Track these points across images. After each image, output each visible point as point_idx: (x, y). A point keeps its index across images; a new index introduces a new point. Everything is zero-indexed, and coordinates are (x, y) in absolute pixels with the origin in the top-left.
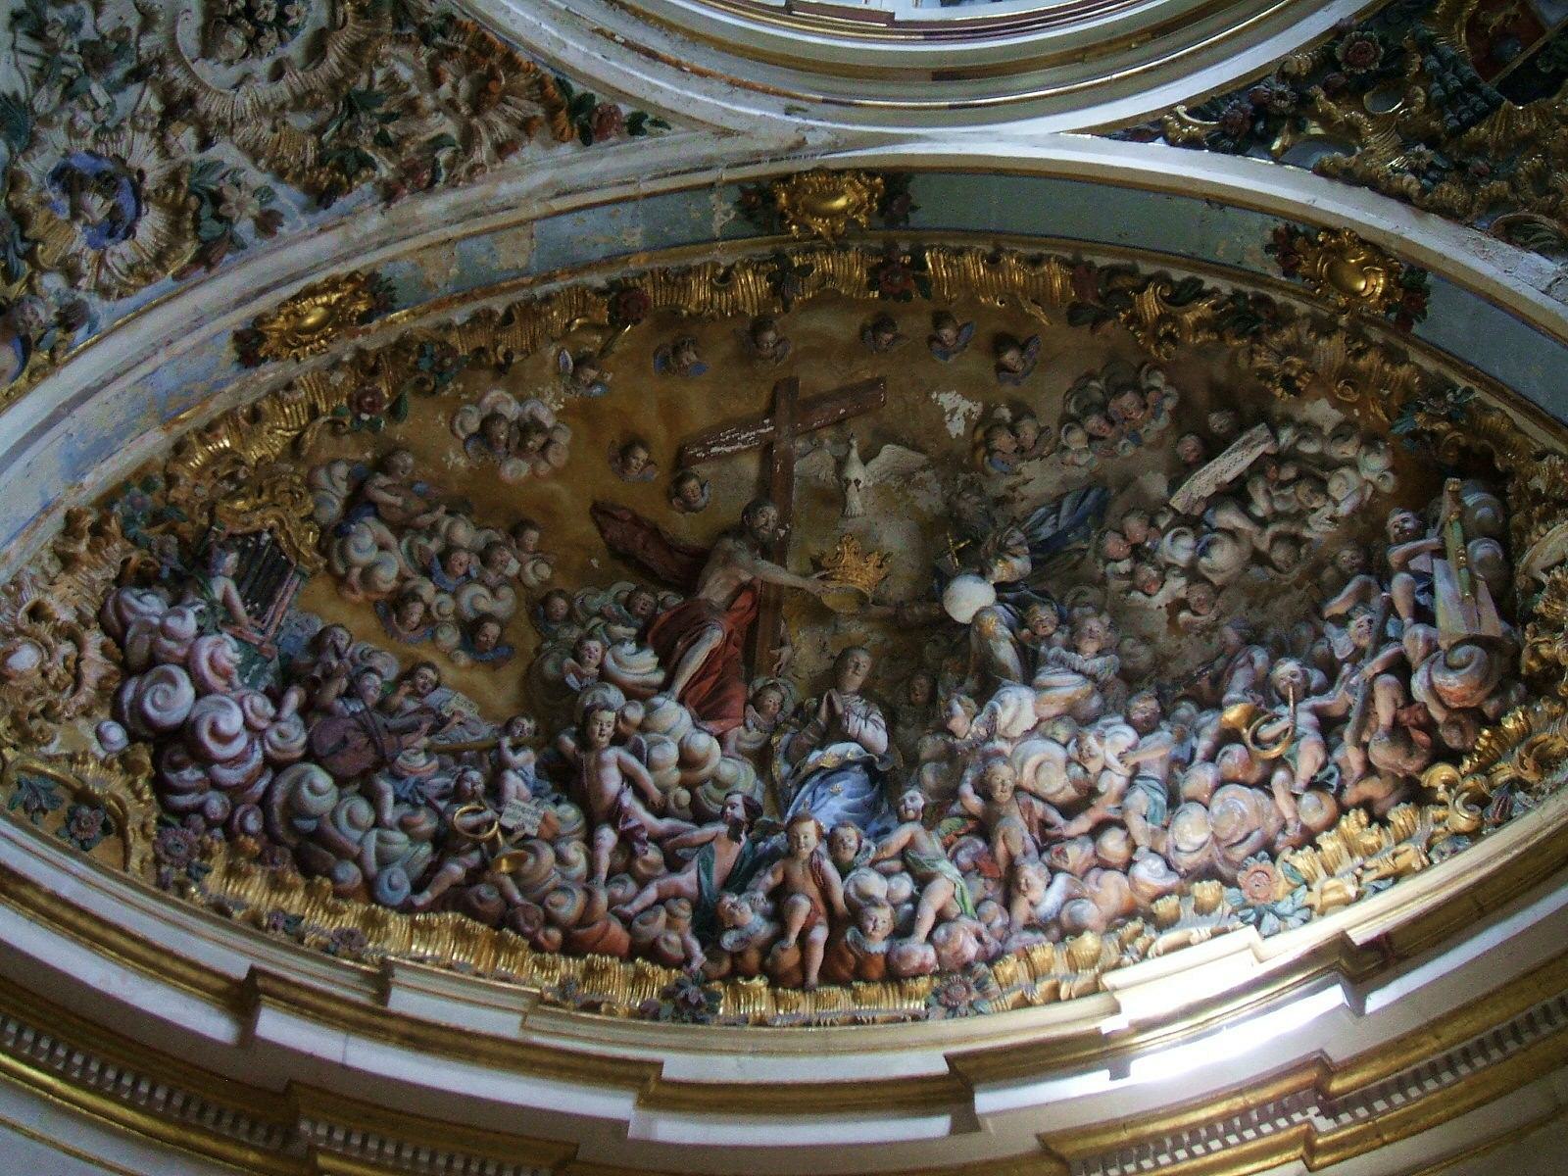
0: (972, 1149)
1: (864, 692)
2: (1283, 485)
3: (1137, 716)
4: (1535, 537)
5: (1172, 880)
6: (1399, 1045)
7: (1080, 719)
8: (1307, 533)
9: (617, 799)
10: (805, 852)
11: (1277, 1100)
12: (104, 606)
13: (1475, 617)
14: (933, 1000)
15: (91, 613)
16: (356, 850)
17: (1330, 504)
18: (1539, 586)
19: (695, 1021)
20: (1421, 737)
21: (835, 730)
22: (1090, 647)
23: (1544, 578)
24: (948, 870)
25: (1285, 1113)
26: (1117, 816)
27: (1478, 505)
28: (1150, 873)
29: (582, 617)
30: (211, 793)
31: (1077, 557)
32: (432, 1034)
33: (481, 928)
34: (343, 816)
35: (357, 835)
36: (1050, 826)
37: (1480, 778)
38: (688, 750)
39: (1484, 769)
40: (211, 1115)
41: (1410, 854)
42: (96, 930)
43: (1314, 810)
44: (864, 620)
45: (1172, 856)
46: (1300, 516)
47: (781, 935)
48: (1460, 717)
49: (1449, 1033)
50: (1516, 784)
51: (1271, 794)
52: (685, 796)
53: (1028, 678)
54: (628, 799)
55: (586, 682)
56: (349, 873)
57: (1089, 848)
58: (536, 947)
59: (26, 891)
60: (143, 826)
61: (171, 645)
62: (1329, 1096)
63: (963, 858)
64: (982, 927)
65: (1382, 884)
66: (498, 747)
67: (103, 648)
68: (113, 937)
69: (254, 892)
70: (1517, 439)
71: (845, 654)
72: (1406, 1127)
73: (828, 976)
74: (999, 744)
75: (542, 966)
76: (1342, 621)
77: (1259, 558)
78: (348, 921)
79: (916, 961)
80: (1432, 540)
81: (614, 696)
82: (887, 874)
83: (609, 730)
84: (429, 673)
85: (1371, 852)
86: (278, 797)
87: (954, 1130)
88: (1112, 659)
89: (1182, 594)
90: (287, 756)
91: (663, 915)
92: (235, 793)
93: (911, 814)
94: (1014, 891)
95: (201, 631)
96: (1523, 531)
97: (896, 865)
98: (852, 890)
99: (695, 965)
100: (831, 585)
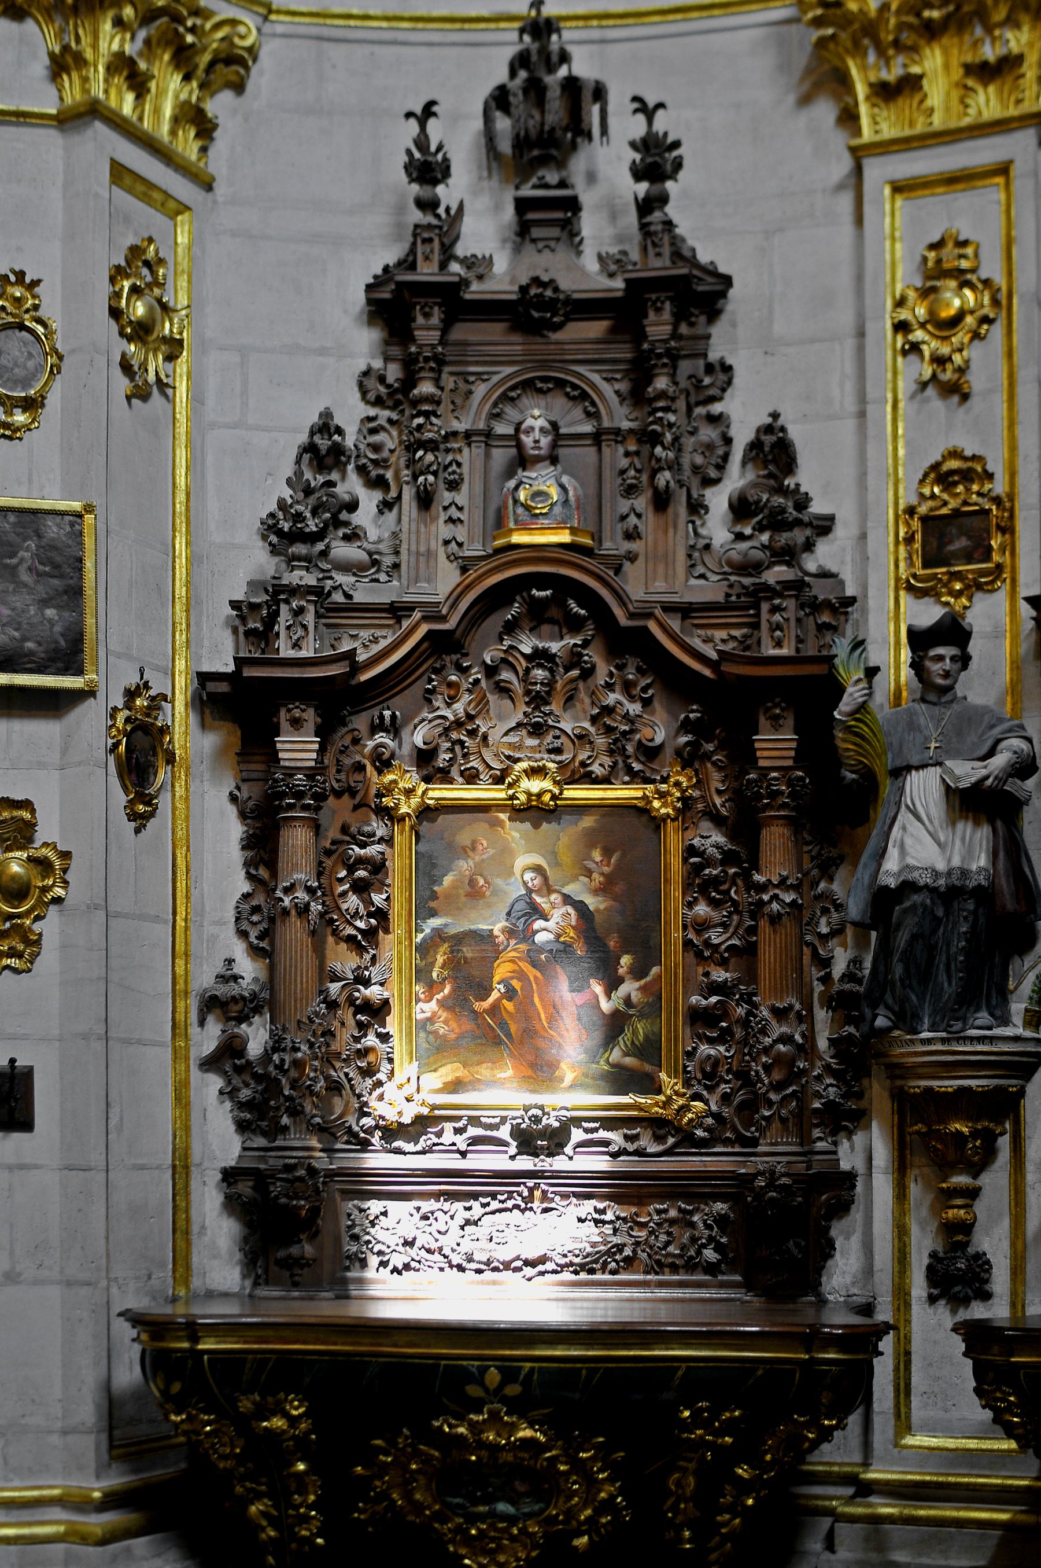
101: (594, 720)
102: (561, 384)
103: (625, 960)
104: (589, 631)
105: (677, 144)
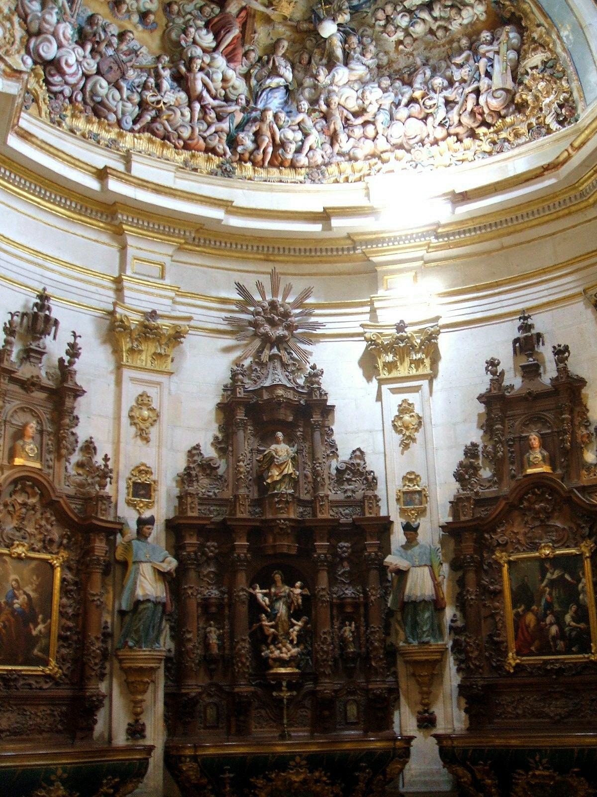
0: (328, 235)
1: (284, 56)
2: (446, 7)
3: (383, 86)
4: (530, 56)
5: (388, 147)
6: (461, 222)
7: (363, 83)
8: (450, 27)
9: (201, 92)
10: (268, 121)
11: (423, 232)
12: (17, 5)
13: (504, 81)
14: (306, 176)
15: (13, 8)
16: (115, 109)
17: (461, 19)
18: (527, 73)
19: (229, 177)
20: (479, 117)
21: (274, 72)
22: (369, 56)
23: (529, 71)
24: (314, 132)
25: (424, 236)
26: (372, 120)
27: (514, 38)
28: (382, 144)
29: (183, 14)
30: (65, 87)
31: (365, 14)
32: (162, 189)
33: (158, 140)
34: (110, 97)
35: (115, 103)
36: (349, 120)
37: (495, 135)
38: (226, 75)
39: (497, 132)
40: (89, 211)
41: (469, 155)
42: (55, 152)
43: (440, 133)
44: (285, 25)
45: (389, 137)
46: (449, 20)
47: (258, 148)
48: (493, 114)
49: (477, 221)
50: (506, 140)
51: (426, 124)
52: (223, 92)
53: (346, 64)
54: (205, 93)
55: (188, 44)
56: (112, 118)
57: (362, 130)
58: (176, 147)
59: (34, 139)
60: (44, 99)
61: (47, 26)
62: (437, 233)
63: (318, 126)
64: (324, 153)
65: (458, 163)
66: (157, 68)
67: (20, 24)
68: (60, 154)
69: (81, 124)
70: (531, 16)
71: (279, 41)
72: (457, 245)
73: (271, 164)
74: (335, 88)
75: (178, 154)
76: (460, 66)
77: (431, 32)
78: (112, 135)
79: (302, 163)
80: (495, 47)
81: (199, 51)
82: (294, 131)
83: (199, 67)
84: (131, 35)
85: (456, 151)
86: (88, 88)
87: (323, 229)
88: (375, 60)
89: (402, 38)
90: (90, 73)
91: (218, 138)
92: (73, 86)
93: (303, 110)
94: (335, 141)
95: (58, 22)
96: (526, 52)
97: (297, 128)
98: (282, 136)
99: (228, 156)
100: (276, 12)
101: (36, 529)
102: (31, 410)
103: (40, 617)
104: (38, 497)
105: (80, 349)
